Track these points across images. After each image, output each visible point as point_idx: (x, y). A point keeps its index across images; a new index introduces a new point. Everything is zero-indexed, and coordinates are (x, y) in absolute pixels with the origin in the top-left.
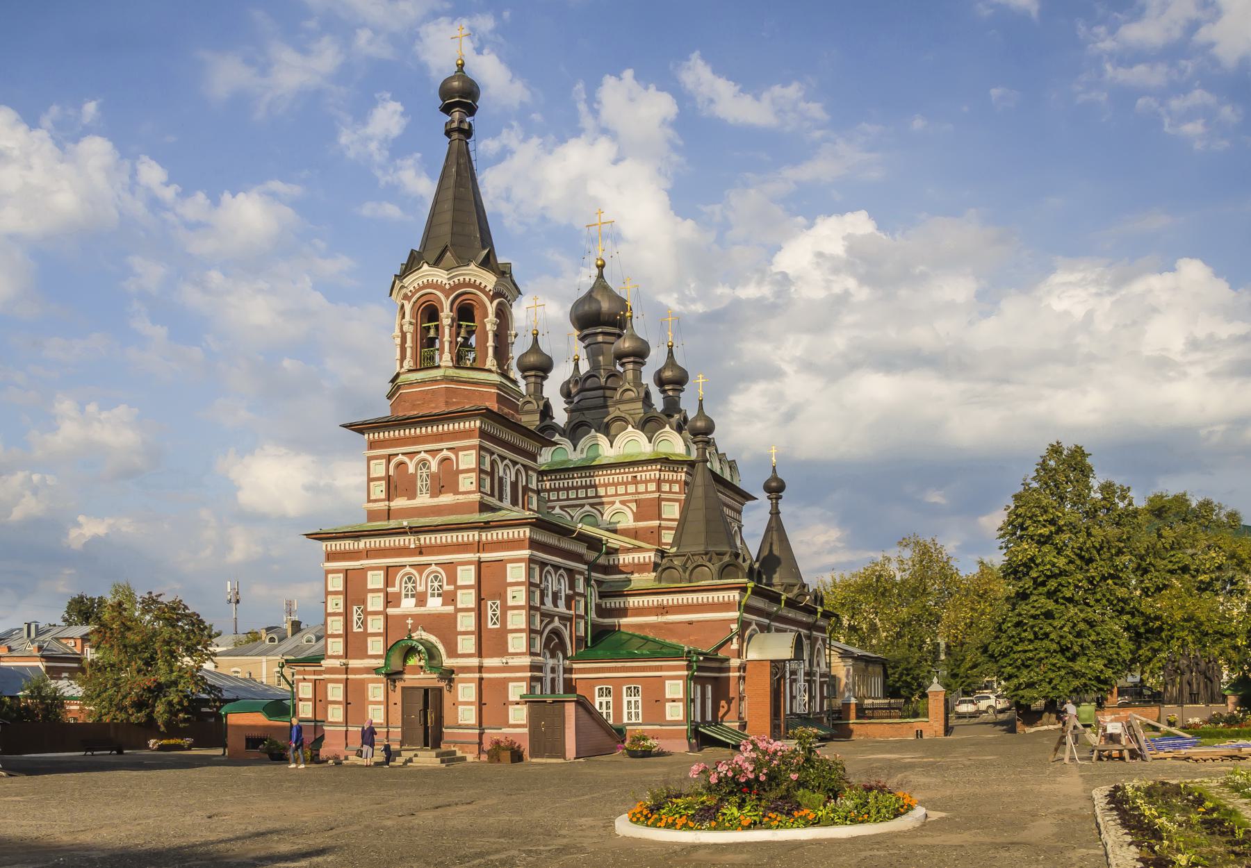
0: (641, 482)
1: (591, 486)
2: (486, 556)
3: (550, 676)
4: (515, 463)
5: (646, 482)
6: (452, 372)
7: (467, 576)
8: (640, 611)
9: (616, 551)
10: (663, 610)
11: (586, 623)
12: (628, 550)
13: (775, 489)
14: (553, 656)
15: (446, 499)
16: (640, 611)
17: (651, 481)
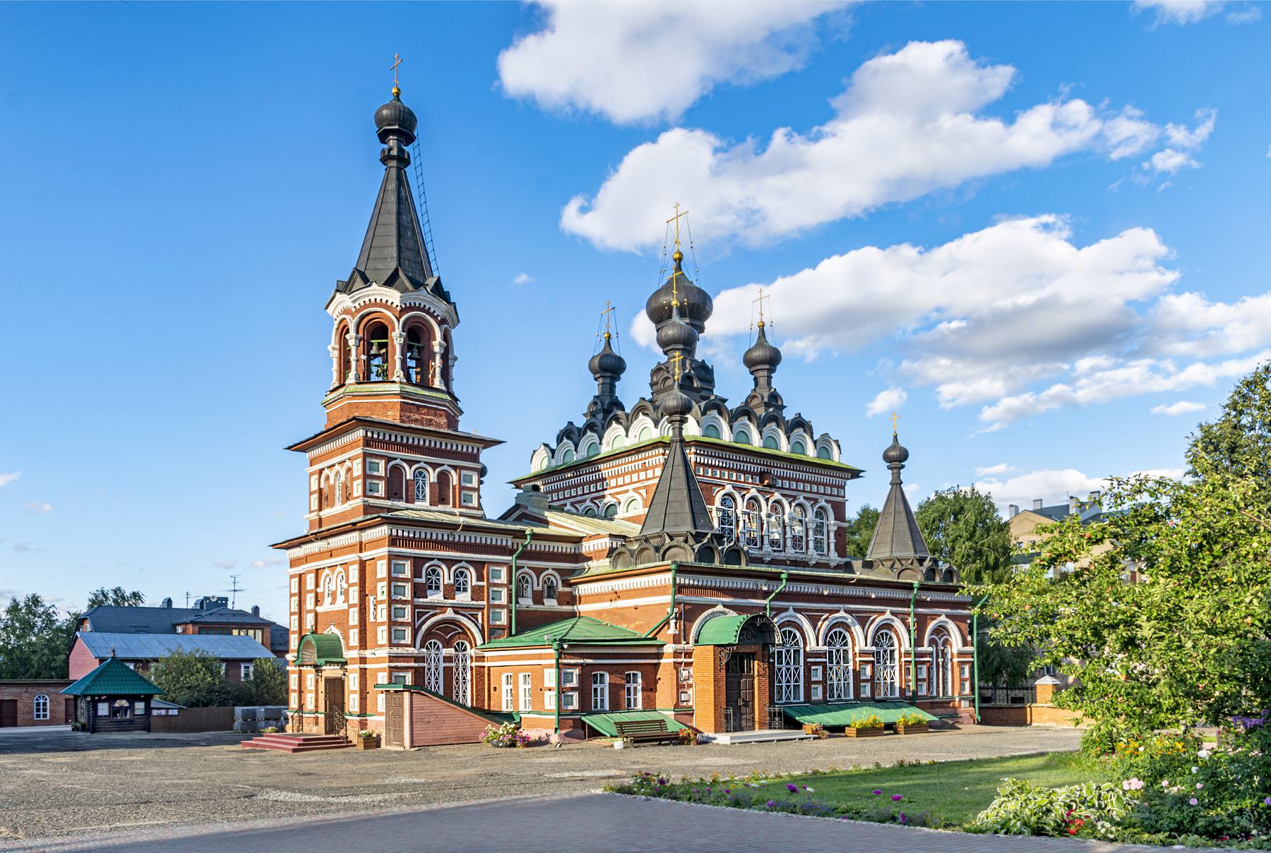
0: (651, 468)
1: (599, 480)
2: (365, 555)
3: (442, 665)
4: (434, 466)
5: (653, 468)
6: (352, 388)
7: (354, 576)
8: (598, 597)
9: (578, 540)
10: (617, 595)
11: (510, 612)
12: (591, 538)
13: (897, 459)
14: (447, 644)
15: (348, 506)
16: (598, 597)
17: (656, 466)
